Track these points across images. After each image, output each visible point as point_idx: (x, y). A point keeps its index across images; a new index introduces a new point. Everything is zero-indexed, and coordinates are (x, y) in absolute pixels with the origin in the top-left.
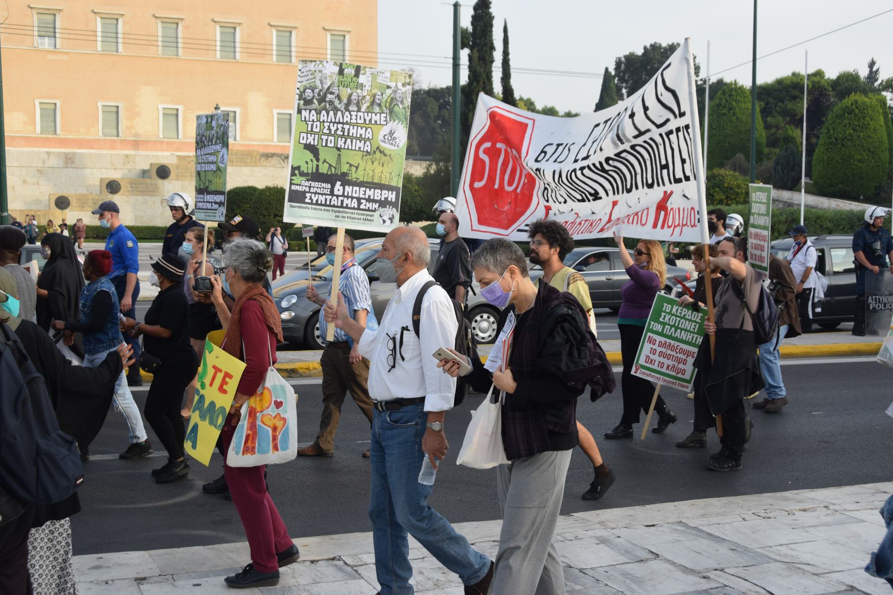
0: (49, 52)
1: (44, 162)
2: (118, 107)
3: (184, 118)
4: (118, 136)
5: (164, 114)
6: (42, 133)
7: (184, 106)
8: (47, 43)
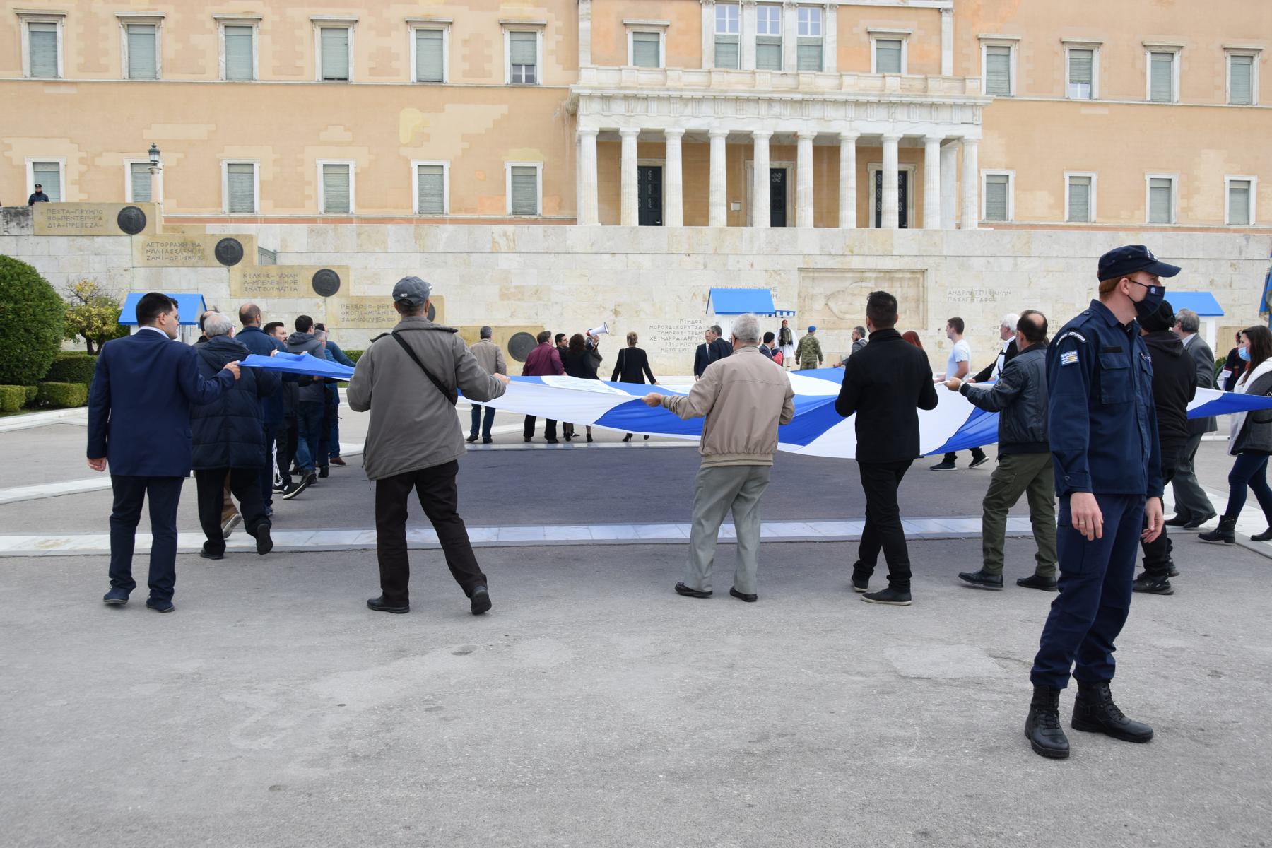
0: (1083, 103)
1: (1241, 252)
2: (1170, 180)
3: (1258, 194)
4: (1169, 222)
5: (1232, 190)
6: (1070, 220)
7: (1259, 178)
8: (1079, 92)
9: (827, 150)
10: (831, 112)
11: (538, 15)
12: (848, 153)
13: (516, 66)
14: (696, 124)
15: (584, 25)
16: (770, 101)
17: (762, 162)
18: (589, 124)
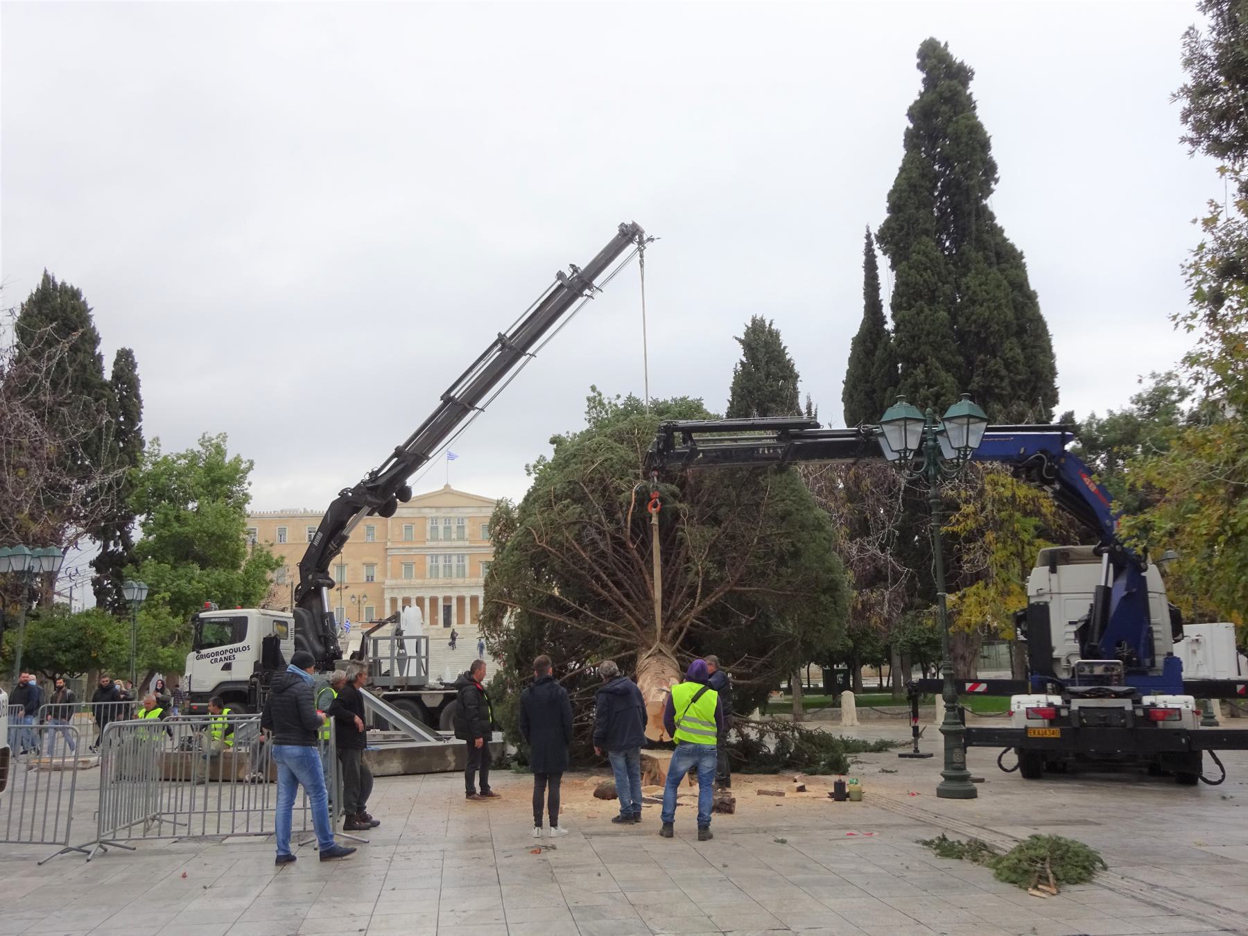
9: (461, 600)
10: (461, 590)
11: (374, 560)
12: (468, 601)
13: (368, 577)
14: (420, 595)
15: (389, 563)
16: (443, 587)
17: (441, 603)
18: (388, 596)
